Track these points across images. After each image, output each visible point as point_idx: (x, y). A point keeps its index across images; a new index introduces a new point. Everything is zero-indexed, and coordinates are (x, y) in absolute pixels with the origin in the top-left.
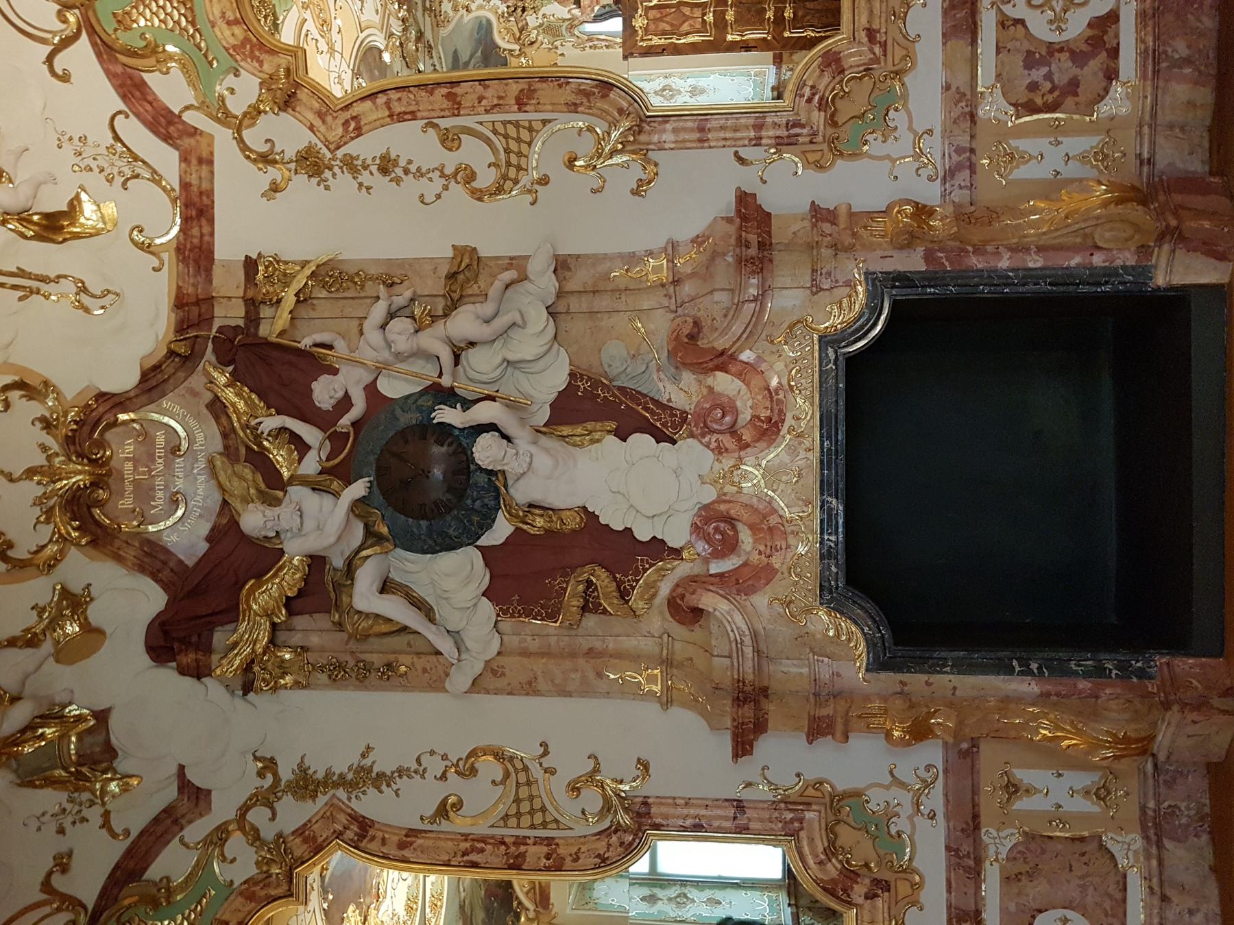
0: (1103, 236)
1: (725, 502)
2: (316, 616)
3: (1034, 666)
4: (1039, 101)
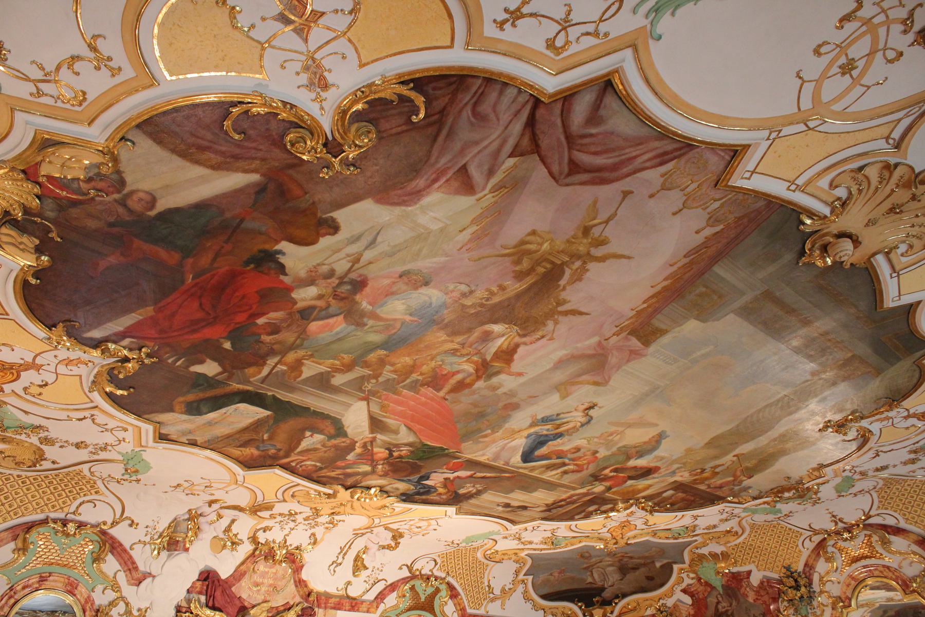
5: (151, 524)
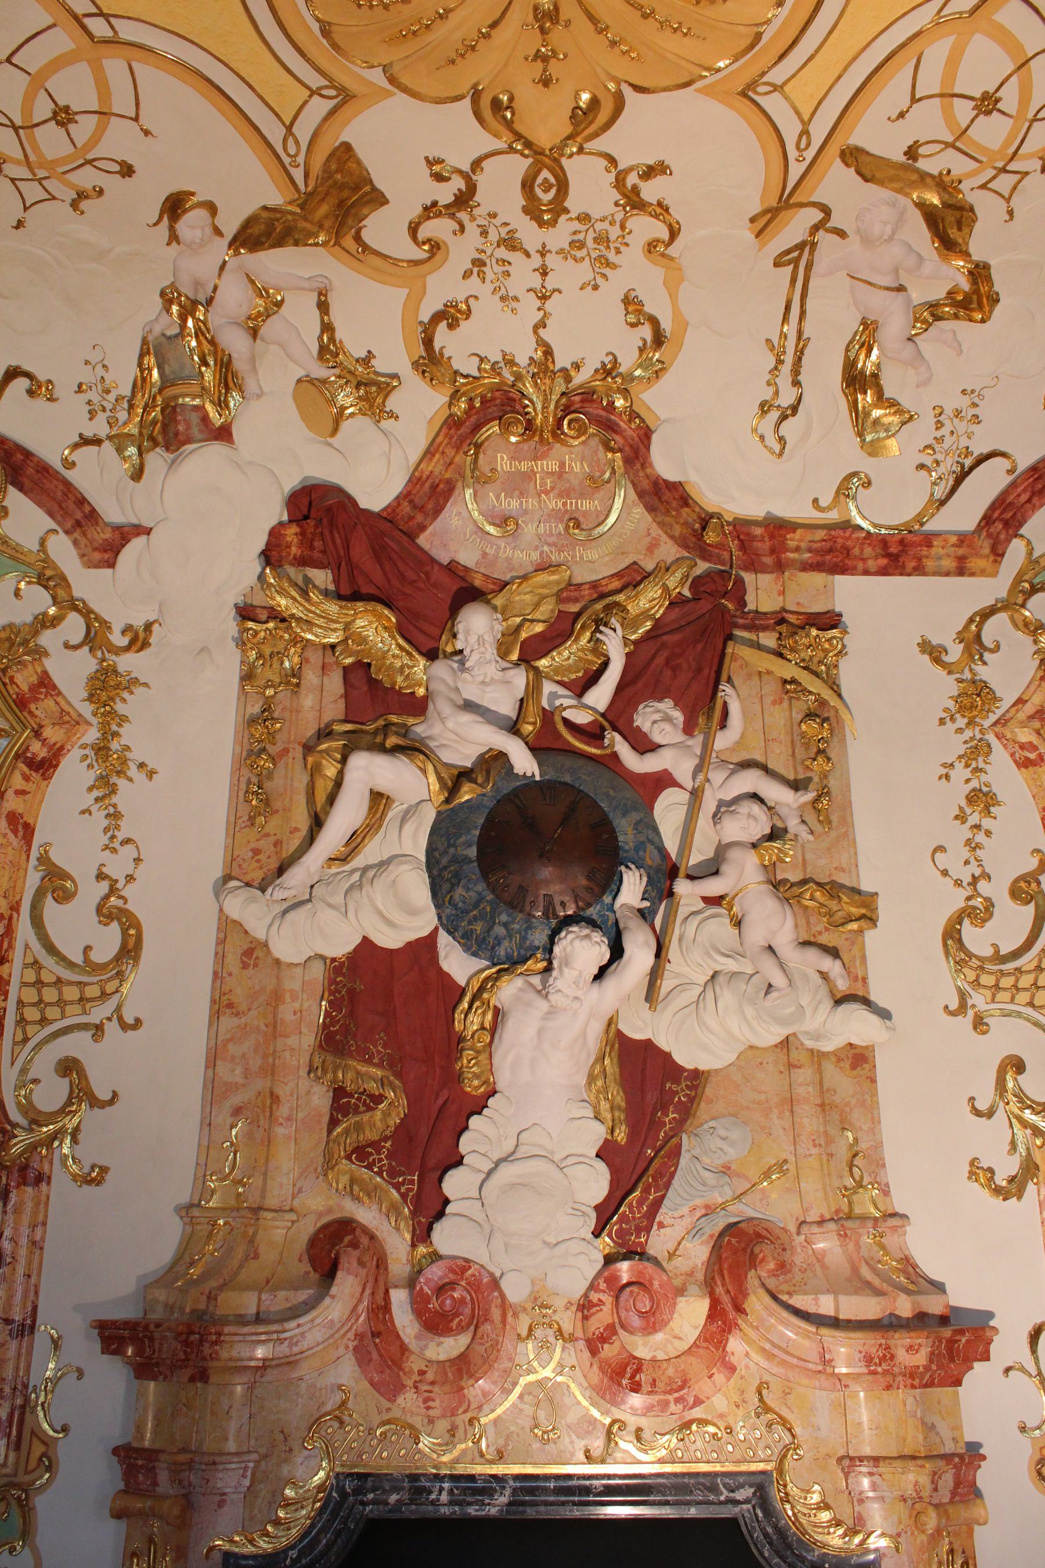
1: (504, 1316)
2: (341, 704)
5: (87, 376)
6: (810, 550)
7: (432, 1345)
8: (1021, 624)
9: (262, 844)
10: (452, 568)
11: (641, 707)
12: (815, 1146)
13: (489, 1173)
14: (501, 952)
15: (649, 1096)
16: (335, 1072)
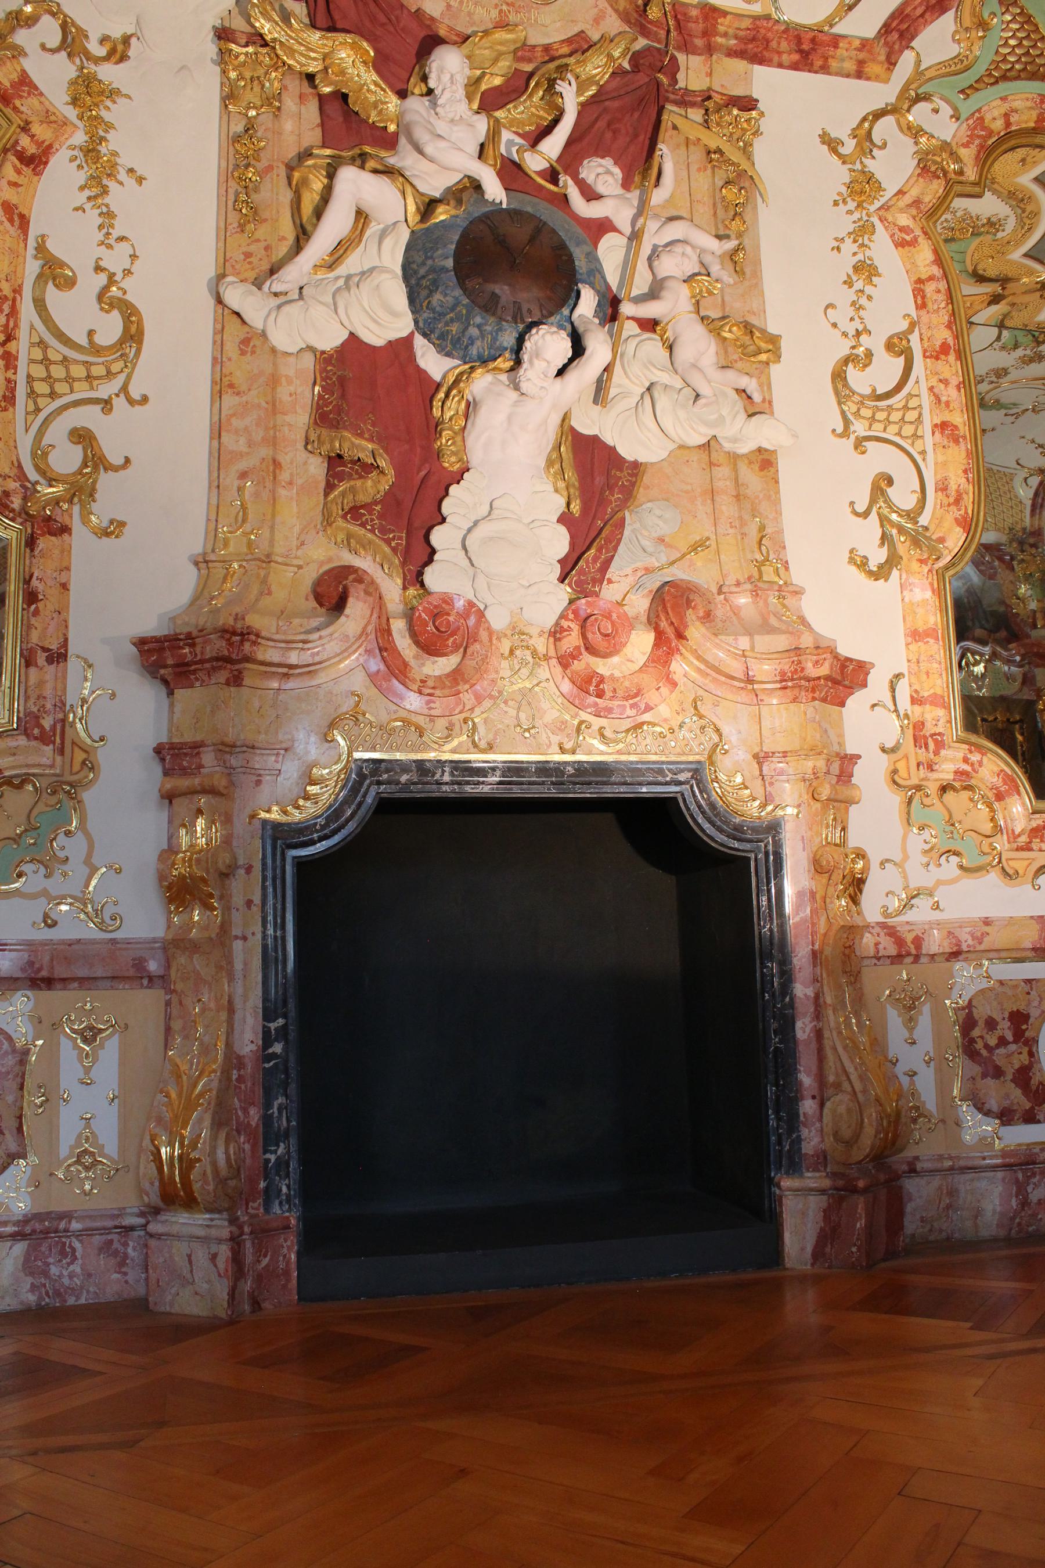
0: (839, 1104)
1: (491, 641)
2: (318, 132)
3: (277, 1048)
4: (976, 1033)
6: (736, 37)
7: (428, 663)
8: (905, 127)
9: (252, 248)
10: (419, 15)
11: (586, 162)
12: (731, 527)
13: (469, 530)
14: (474, 351)
15: (598, 479)
16: (332, 442)
